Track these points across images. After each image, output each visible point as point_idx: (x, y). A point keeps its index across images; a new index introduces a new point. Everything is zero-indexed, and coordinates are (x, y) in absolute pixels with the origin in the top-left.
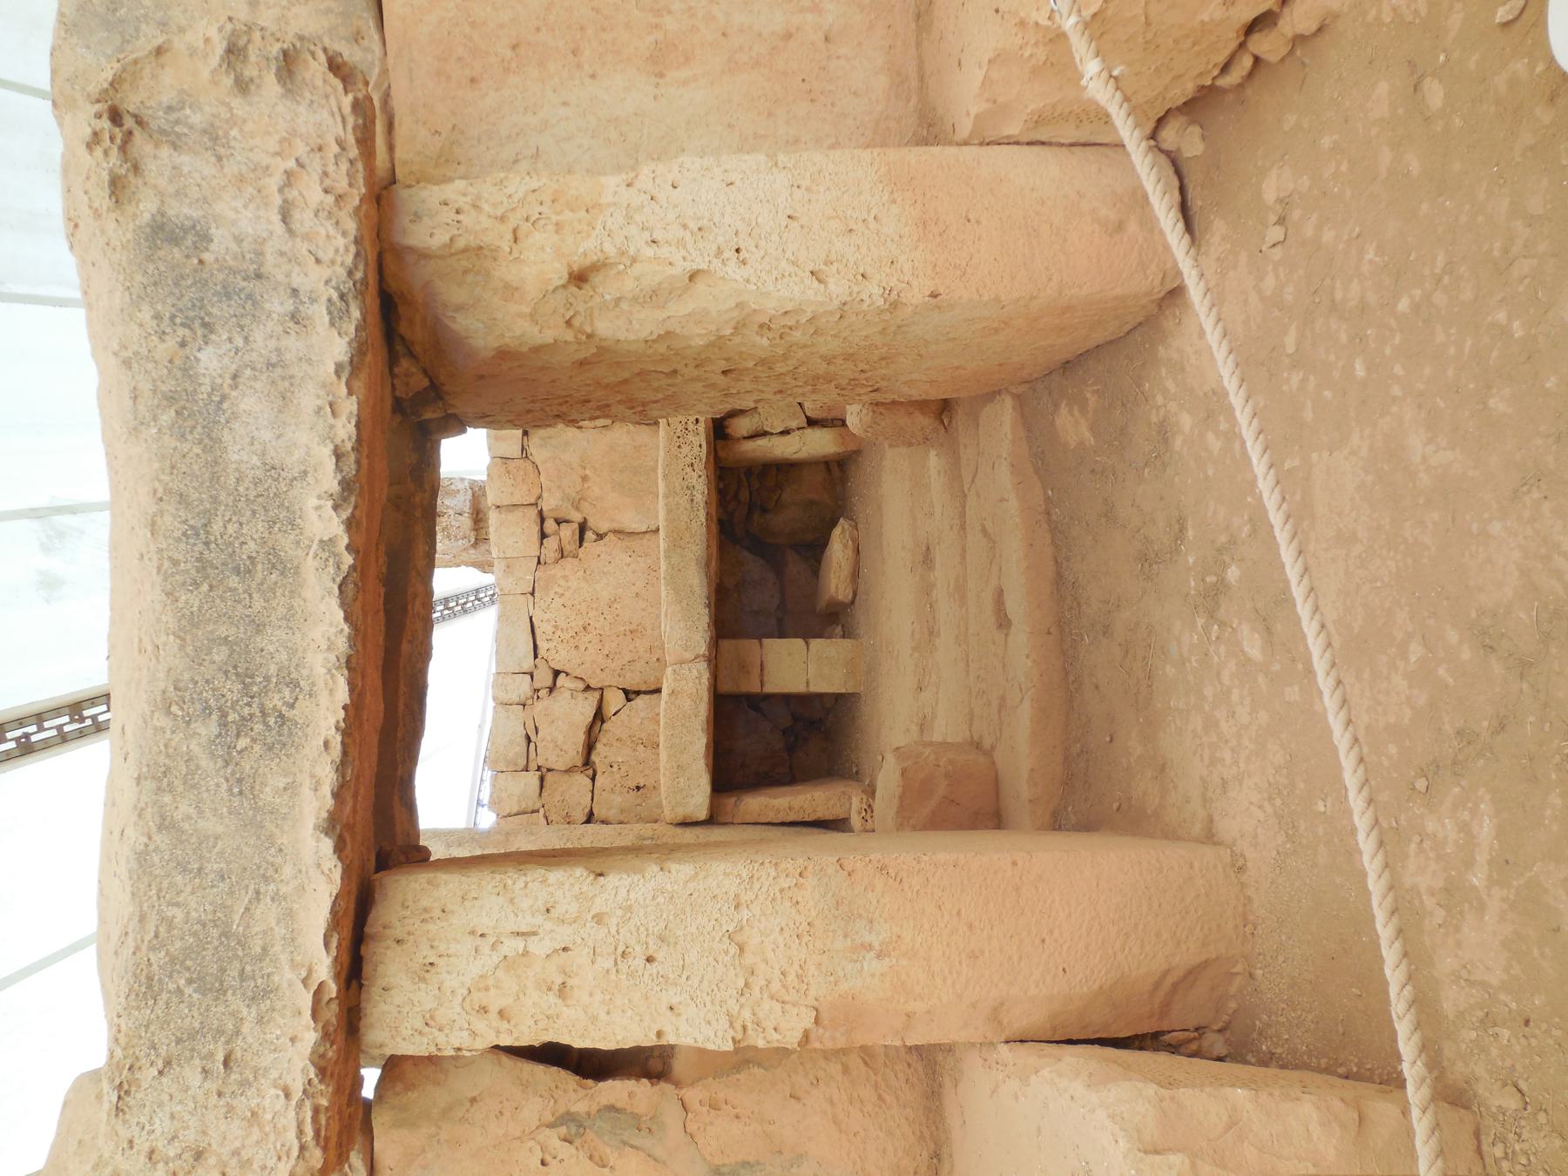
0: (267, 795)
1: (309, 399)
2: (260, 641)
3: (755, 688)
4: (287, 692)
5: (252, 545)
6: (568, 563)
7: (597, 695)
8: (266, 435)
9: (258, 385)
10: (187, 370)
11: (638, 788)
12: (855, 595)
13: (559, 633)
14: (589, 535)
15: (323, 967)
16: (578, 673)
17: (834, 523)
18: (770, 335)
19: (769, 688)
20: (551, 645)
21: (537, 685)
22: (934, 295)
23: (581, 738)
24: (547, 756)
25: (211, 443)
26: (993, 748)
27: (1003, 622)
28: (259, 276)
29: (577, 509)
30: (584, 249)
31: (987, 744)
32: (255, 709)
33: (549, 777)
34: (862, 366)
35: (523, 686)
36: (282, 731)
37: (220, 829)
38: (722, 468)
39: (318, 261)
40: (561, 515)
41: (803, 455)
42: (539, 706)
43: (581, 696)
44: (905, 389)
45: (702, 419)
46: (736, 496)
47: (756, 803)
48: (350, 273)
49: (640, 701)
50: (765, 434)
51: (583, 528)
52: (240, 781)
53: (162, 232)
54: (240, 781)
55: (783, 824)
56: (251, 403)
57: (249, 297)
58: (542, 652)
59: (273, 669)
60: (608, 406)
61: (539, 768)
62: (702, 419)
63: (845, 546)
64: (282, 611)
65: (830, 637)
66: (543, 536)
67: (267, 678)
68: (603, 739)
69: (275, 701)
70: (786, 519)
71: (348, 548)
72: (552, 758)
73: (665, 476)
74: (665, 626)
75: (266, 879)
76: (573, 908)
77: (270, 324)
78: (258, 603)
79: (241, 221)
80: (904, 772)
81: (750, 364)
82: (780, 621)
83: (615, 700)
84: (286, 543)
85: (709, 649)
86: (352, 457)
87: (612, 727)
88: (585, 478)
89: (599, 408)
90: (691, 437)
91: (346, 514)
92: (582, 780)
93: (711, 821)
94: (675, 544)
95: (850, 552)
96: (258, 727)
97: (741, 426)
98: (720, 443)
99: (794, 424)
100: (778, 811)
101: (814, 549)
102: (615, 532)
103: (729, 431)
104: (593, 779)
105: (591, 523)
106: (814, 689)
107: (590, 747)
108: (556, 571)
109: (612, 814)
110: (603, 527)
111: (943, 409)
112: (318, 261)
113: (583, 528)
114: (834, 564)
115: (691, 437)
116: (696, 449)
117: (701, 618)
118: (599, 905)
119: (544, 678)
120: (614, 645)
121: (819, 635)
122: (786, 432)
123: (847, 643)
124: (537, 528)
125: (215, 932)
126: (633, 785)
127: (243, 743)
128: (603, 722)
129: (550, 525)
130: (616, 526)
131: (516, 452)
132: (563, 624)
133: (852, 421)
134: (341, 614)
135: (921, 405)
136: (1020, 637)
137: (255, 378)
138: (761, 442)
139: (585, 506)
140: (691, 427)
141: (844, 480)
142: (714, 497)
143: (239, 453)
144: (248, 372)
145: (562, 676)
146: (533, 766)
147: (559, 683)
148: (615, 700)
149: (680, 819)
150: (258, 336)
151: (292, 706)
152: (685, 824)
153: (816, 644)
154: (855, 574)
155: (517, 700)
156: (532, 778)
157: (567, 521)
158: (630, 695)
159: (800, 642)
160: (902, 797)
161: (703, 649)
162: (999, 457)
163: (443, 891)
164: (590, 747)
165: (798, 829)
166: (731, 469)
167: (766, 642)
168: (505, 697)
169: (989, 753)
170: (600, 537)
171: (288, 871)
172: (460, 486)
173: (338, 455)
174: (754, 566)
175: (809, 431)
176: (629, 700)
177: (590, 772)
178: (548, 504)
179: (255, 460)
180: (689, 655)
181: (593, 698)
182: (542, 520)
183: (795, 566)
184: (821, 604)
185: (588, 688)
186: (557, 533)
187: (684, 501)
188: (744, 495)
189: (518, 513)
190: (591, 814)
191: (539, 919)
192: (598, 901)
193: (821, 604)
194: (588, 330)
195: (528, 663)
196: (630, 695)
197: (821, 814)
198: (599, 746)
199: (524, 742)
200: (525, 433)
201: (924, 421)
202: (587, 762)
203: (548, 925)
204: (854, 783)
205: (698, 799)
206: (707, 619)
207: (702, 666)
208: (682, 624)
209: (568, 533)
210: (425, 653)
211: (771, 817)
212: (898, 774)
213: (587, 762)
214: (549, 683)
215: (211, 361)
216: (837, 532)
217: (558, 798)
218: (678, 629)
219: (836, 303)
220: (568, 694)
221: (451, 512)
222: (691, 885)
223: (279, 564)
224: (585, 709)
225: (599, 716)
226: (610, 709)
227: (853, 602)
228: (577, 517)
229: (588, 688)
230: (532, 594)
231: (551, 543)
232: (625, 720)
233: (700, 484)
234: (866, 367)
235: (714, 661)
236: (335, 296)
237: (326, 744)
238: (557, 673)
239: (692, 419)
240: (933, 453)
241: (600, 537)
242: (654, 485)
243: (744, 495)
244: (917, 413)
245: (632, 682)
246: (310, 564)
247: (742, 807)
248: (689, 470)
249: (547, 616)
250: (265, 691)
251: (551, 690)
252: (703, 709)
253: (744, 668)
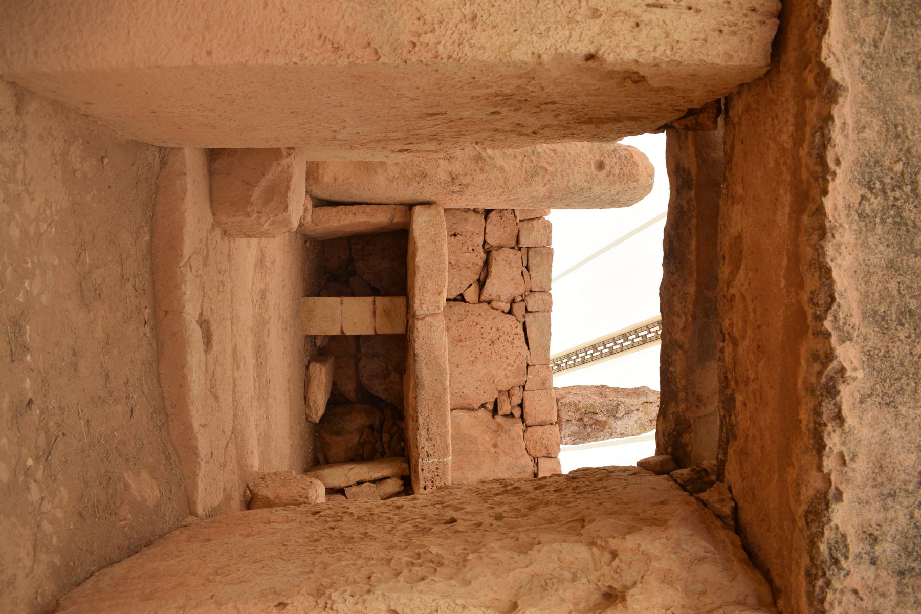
0: (876, 124)
1: (861, 467)
2: (890, 253)
3: (379, 299)
4: (868, 210)
5: (902, 336)
6: (504, 387)
7: (483, 298)
8: (895, 433)
9: (903, 476)
11: (455, 235)
12: (307, 368)
13: (510, 339)
14: (490, 407)
16: (496, 312)
17: (323, 419)
18: (429, 556)
19: (370, 299)
20: (515, 331)
21: (523, 304)
22: (282, 605)
23: (494, 269)
24: (515, 257)
26: (213, 227)
27: (204, 324)
28: (901, 573)
29: (499, 424)
31: (218, 232)
32: (891, 195)
33: (513, 244)
34: (335, 533)
35: (532, 304)
37: (908, 98)
38: (403, 456)
39: (855, 592)
40: (510, 420)
41: (347, 467)
42: (521, 290)
43: (494, 297)
44: (291, 515)
45: (422, 490)
46: (391, 437)
47: (380, 218)
48: (828, 584)
50: (375, 481)
51: (495, 412)
52: (898, 136)
54: (898, 136)
55: (360, 204)
57: (910, 554)
58: (521, 326)
59: (879, 230)
60: (536, 489)
61: (520, 249)
62: (422, 490)
63: (315, 402)
64: (874, 280)
65: (325, 336)
66: (521, 406)
67: (883, 221)
68: (478, 268)
69: (876, 202)
70: (356, 422)
71: (829, 335)
72: (511, 256)
73: (447, 447)
74: (445, 341)
75: (871, 56)
76: (617, 25)
77: (893, 531)
78: (893, 285)
80: (286, 209)
81: (435, 529)
82: (358, 350)
83: (471, 294)
84: (874, 340)
85: (414, 325)
86: (825, 418)
88: (495, 446)
89: (543, 486)
90: (429, 476)
91: (834, 365)
92: (492, 241)
93: (410, 206)
94: (439, 399)
95: (312, 398)
96: (887, 180)
97: (393, 485)
98: (406, 473)
99: (354, 489)
100: (364, 212)
101: (335, 401)
102: (472, 409)
103: (401, 482)
104: (485, 241)
105: (489, 416)
106: (338, 299)
107: (487, 263)
108: (513, 381)
109: (472, 217)
110: (481, 413)
111: (251, 502)
112: (855, 592)
113: (495, 412)
114: (323, 389)
115: (429, 476)
116: (425, 468)
117: (420, 345)
118: (595, 26)
119: (519, 309)
120: (473, 331)
121: (332, 338)
122: (359, 483)
123: (313, 332)
124: (527, 410)
125: (904, 17)
126: (459, 237)
127: (899, 167)
128: (479, 280)
129: (517, 413)
130: (473, 414)
131: (542, 463)
132: (507, 344)
133: (322, 491)
134: (835, 274)
135: (269, 504)
136: (191, 313)
137: (905, 482)
138: (377, 475)
139: (494, 427)
140: (429, 484)
141: (315, 451)
142: (410, 433)
144: (911, 487)
145: (506, 311)
146: (524, 251)
147: (508, 306)
148: (471, 294)
149: (433, 207)
150: (902, 520)
151: (863, 197)
152: (428, 203)
153: (336, 332)
154: (307, 382)
155: (537, 294)
156: (524, 242)
157: (505, 416)
158: (461, 298)
159: (347, 333)
160: (288, 188)
161: (419, 324)
162: (207, 462)
163: (721, 48)
164: (487, 263)
165: (350, 200)
166: (396, 456)
167: (371, 332)
168: (543, 296)
169: (217, 224)
170: (483, 406)
171: (856, 61)
172: (568, 439)
173: (839, 418)
174: (377, 388)
175: (343, 485)
176: (461, 295)
177: (486, 246)
178: (520, 426)
179: (903, 410)
180: (429, 319)
181: (486, 296)
182: (522, 416)
183: (349, 388)
184: (331, 361)
185: (489, 302)
186: (513, 407)
187: (434, 429)
188: (386, 437)
189: (538, 420)
190: (486, 219)
191: (646, 17)
192: (596, 30)
193: (331, 361)
194: (595, 549)
195: (529, 319)
196: (461, 298)
197: (333, 210)
198: (481, 264)
199: (530, 265)
200: (536, 475)
201: (265, 492)
202: (488, 253)
203: (637, 11)
204: (308, 233)
205: (421, 221)
206: (416, 346)
207: (419, 312)
208: (434, 342)
209: (505, 408)
210: (667, 291)
211: (368, 209)
212: (290, 207)
214: (515, 306)
216: (321, 412)
217: (507, 229)
218: (435, 337)
219: (378, 592)
220: (503, 298)
221: (574, 422)
222: (515, 39)
224: (491, 289)
225: (481, 284)
226: (474, 289)
227: (309, 362)
228: (499, 419)
229: (489, 302)
230: (528, 365)
231: (516, 400)
232: (465, 281)
233: (423, 442)
234: (331, 532)
235: (409, 315)
236: (843, 563)
237: (838, 162)
238: (510, 312)
239: (428, 489)
240: (256, 469)
241: (483, 406)
242: (452, 443)
243: (386, 437)
244: (272, 498)
245: (459, 307)
246: (856, 320)
247: (389, 215)
248: (431, 452)
249: (519, 350)
250: (885, 211)
251: (513, 302)
252: (418, 282)
253: (387, 313)
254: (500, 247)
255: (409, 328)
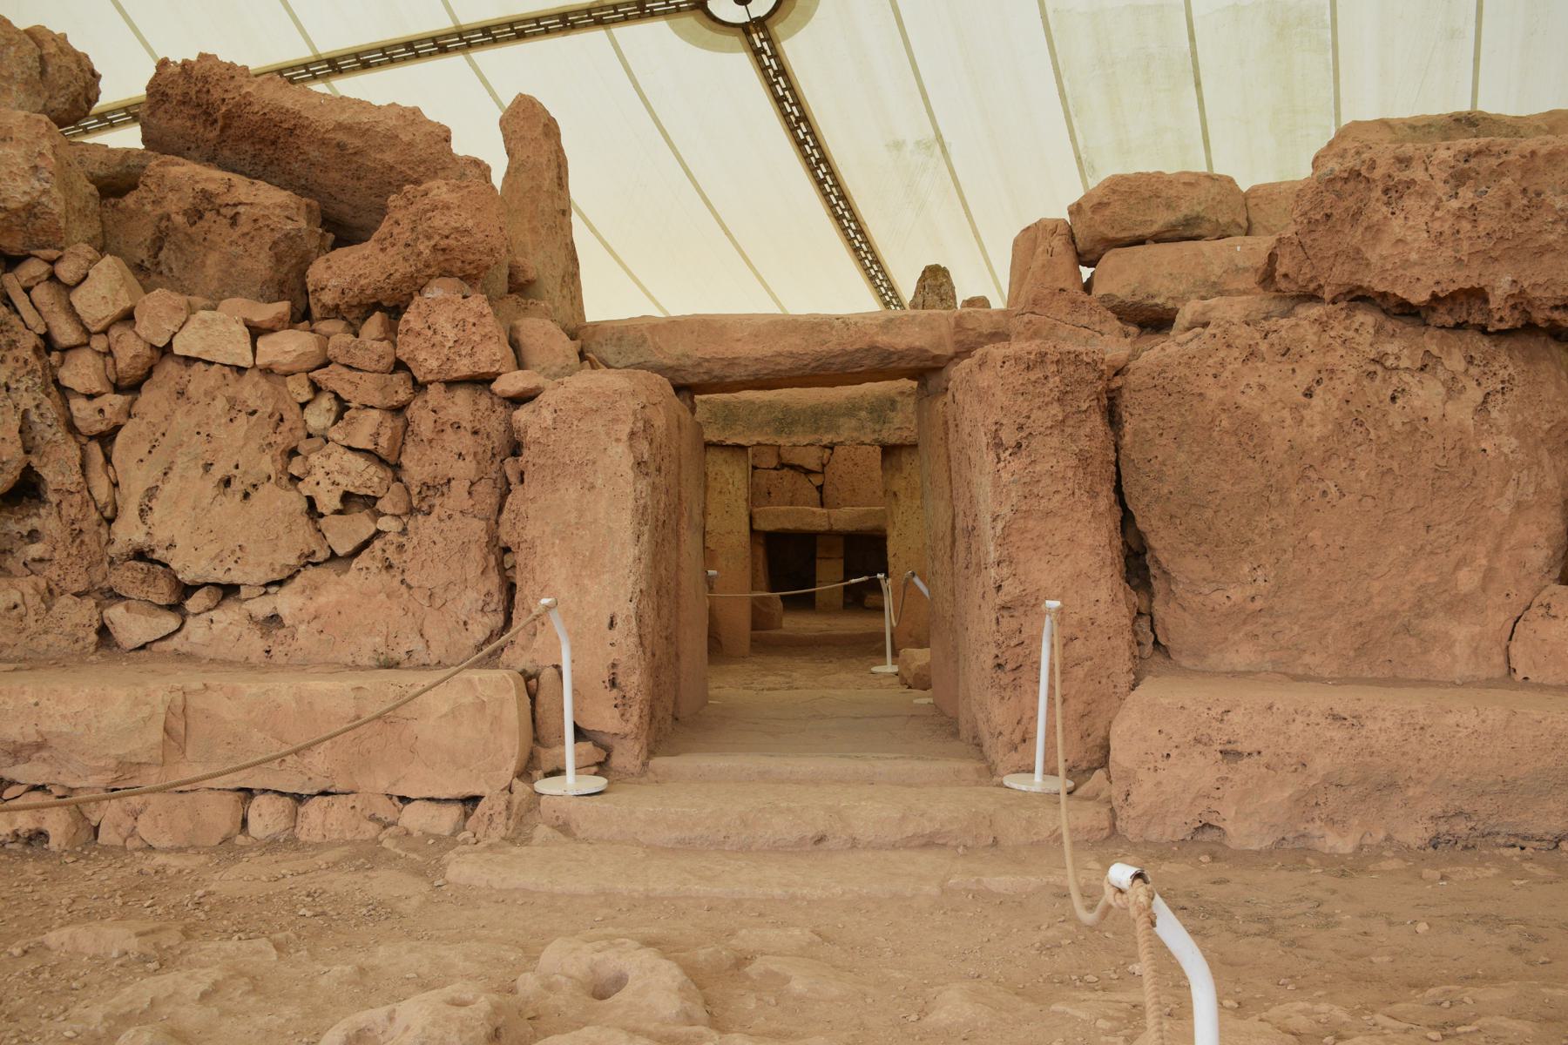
10: (860, 409)
15: (728, 442)
25: (844, 415)
30: (901, 496)
36: (779, 431)
49: (816, 494)
53: (893, 402)
56: (854, 422)
79: (897, 419)
83: (817, 480)
87: (802, 480)
92: (774, 463)
93: (752, 531)
107: (792, 467)
143: (842, 420)
148: (817, 480)
158: (820, 488)
181: (818, 468)
196: (820, 488)
202: (783, 465)
205: (763, 525)
213: (783, 465)
215: (863, 414)
223: (817, 429)
225: (808, 472)
232: (806, 487)
235: (830, 533)
245: (828, 490)
252: (806, 528)
254: (779, 455)
255: (838, 534)
